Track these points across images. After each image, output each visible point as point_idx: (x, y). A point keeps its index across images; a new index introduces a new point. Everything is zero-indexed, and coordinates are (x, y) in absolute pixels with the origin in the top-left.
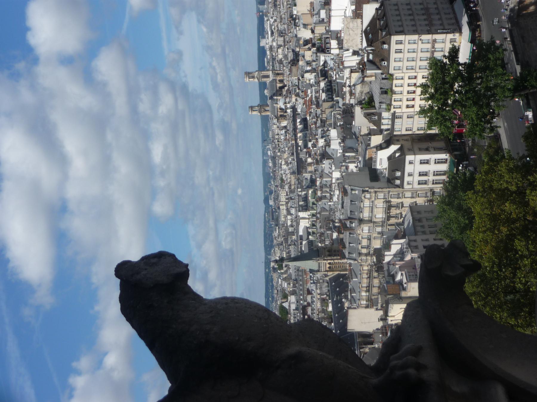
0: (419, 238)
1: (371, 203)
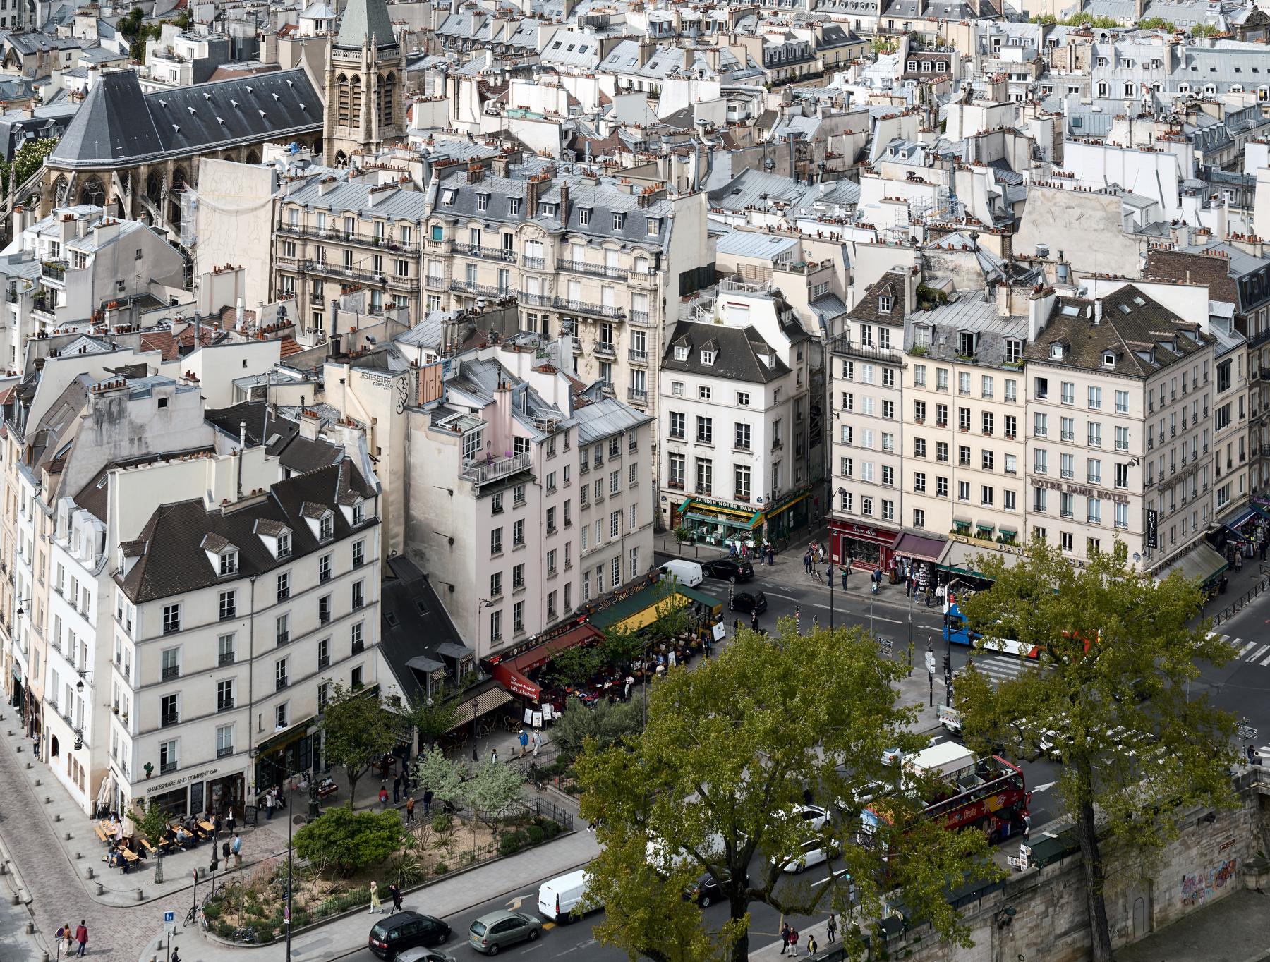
0: (573, 458)
1: (615, 274)
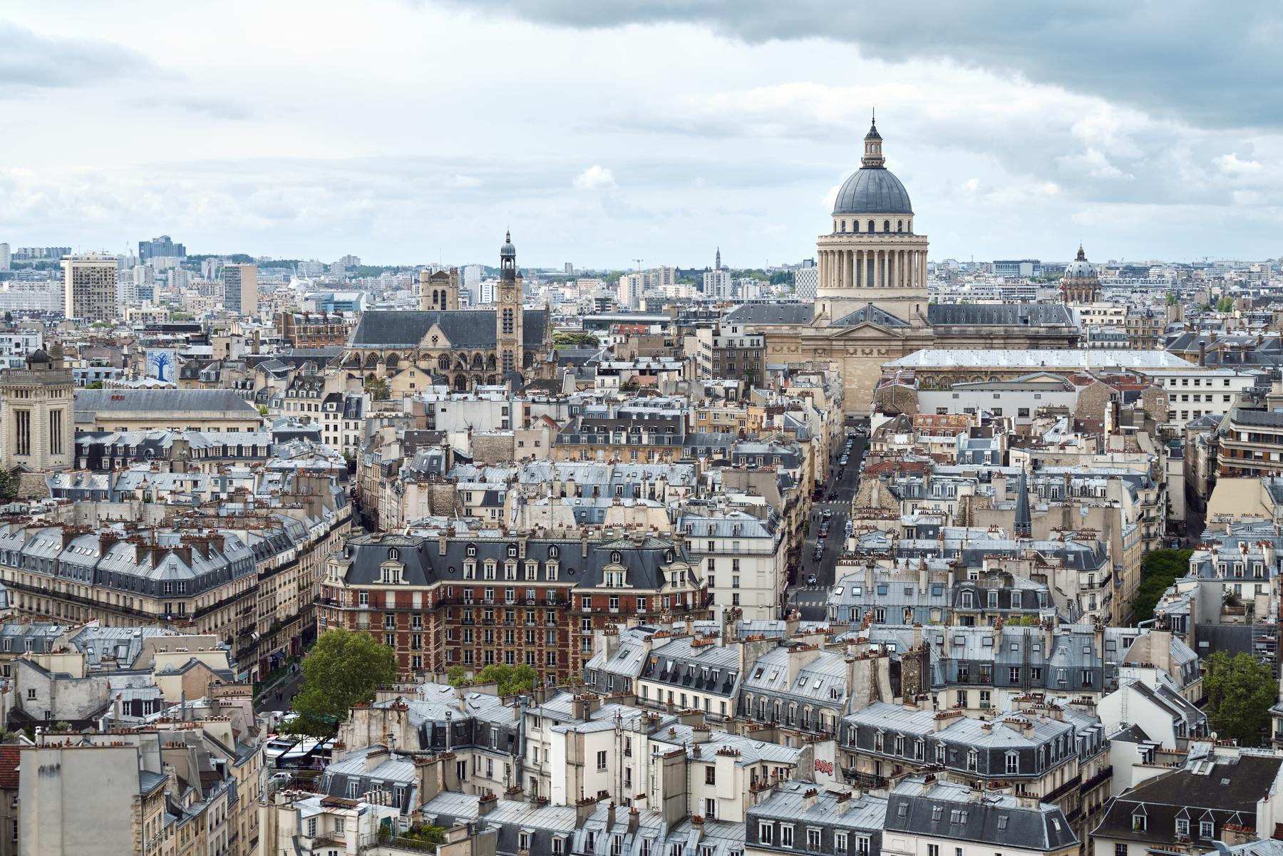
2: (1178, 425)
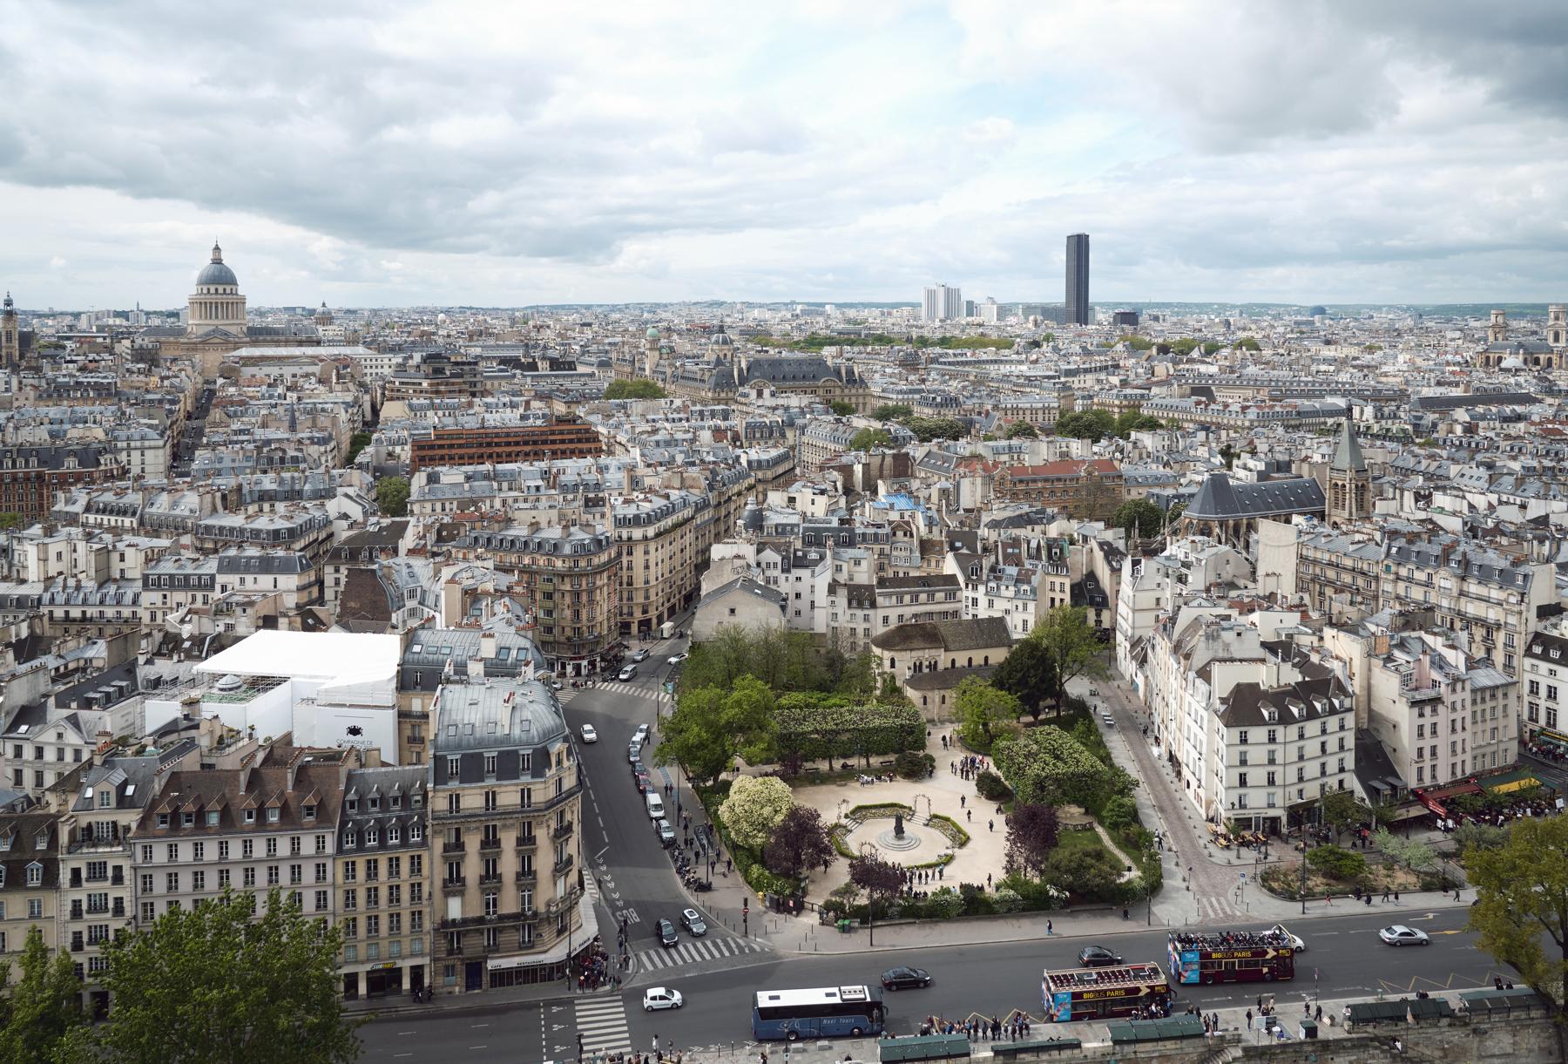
0: (1467, 695)
2: (368, 379)
